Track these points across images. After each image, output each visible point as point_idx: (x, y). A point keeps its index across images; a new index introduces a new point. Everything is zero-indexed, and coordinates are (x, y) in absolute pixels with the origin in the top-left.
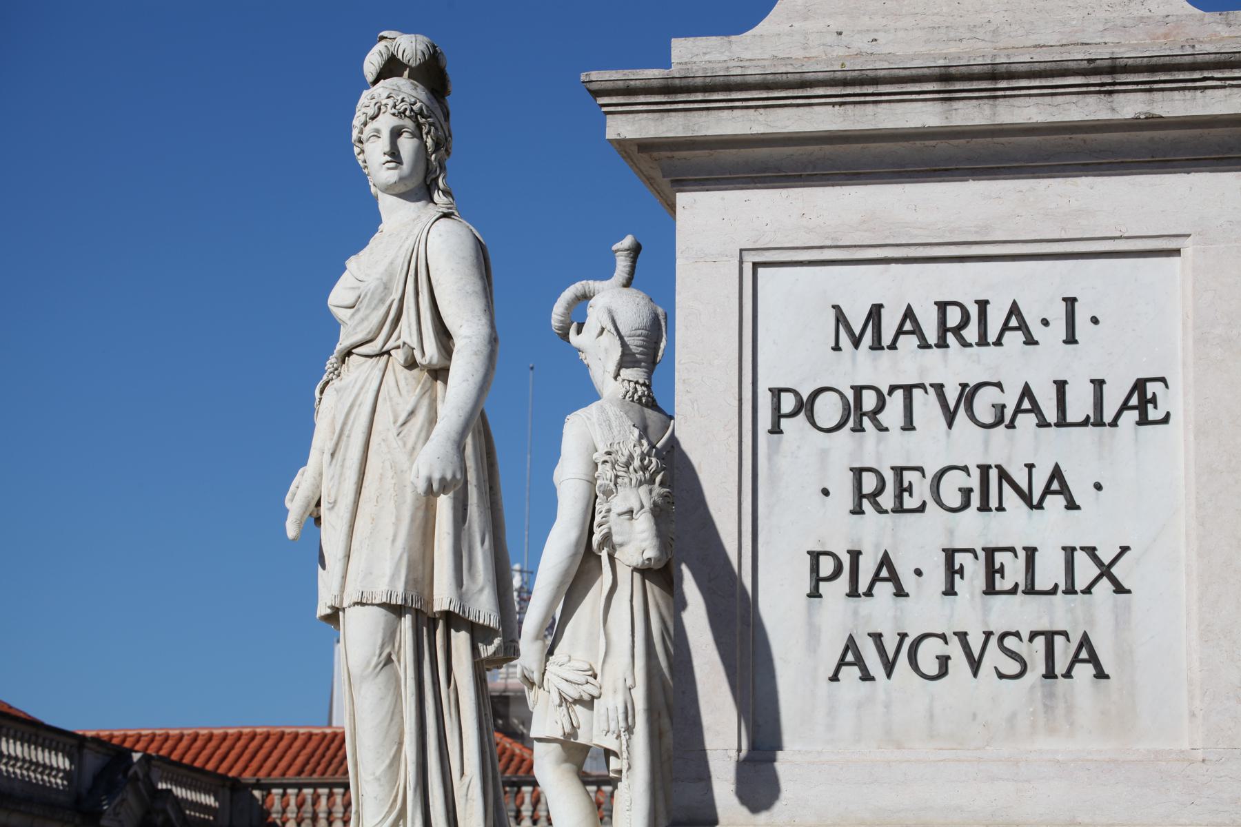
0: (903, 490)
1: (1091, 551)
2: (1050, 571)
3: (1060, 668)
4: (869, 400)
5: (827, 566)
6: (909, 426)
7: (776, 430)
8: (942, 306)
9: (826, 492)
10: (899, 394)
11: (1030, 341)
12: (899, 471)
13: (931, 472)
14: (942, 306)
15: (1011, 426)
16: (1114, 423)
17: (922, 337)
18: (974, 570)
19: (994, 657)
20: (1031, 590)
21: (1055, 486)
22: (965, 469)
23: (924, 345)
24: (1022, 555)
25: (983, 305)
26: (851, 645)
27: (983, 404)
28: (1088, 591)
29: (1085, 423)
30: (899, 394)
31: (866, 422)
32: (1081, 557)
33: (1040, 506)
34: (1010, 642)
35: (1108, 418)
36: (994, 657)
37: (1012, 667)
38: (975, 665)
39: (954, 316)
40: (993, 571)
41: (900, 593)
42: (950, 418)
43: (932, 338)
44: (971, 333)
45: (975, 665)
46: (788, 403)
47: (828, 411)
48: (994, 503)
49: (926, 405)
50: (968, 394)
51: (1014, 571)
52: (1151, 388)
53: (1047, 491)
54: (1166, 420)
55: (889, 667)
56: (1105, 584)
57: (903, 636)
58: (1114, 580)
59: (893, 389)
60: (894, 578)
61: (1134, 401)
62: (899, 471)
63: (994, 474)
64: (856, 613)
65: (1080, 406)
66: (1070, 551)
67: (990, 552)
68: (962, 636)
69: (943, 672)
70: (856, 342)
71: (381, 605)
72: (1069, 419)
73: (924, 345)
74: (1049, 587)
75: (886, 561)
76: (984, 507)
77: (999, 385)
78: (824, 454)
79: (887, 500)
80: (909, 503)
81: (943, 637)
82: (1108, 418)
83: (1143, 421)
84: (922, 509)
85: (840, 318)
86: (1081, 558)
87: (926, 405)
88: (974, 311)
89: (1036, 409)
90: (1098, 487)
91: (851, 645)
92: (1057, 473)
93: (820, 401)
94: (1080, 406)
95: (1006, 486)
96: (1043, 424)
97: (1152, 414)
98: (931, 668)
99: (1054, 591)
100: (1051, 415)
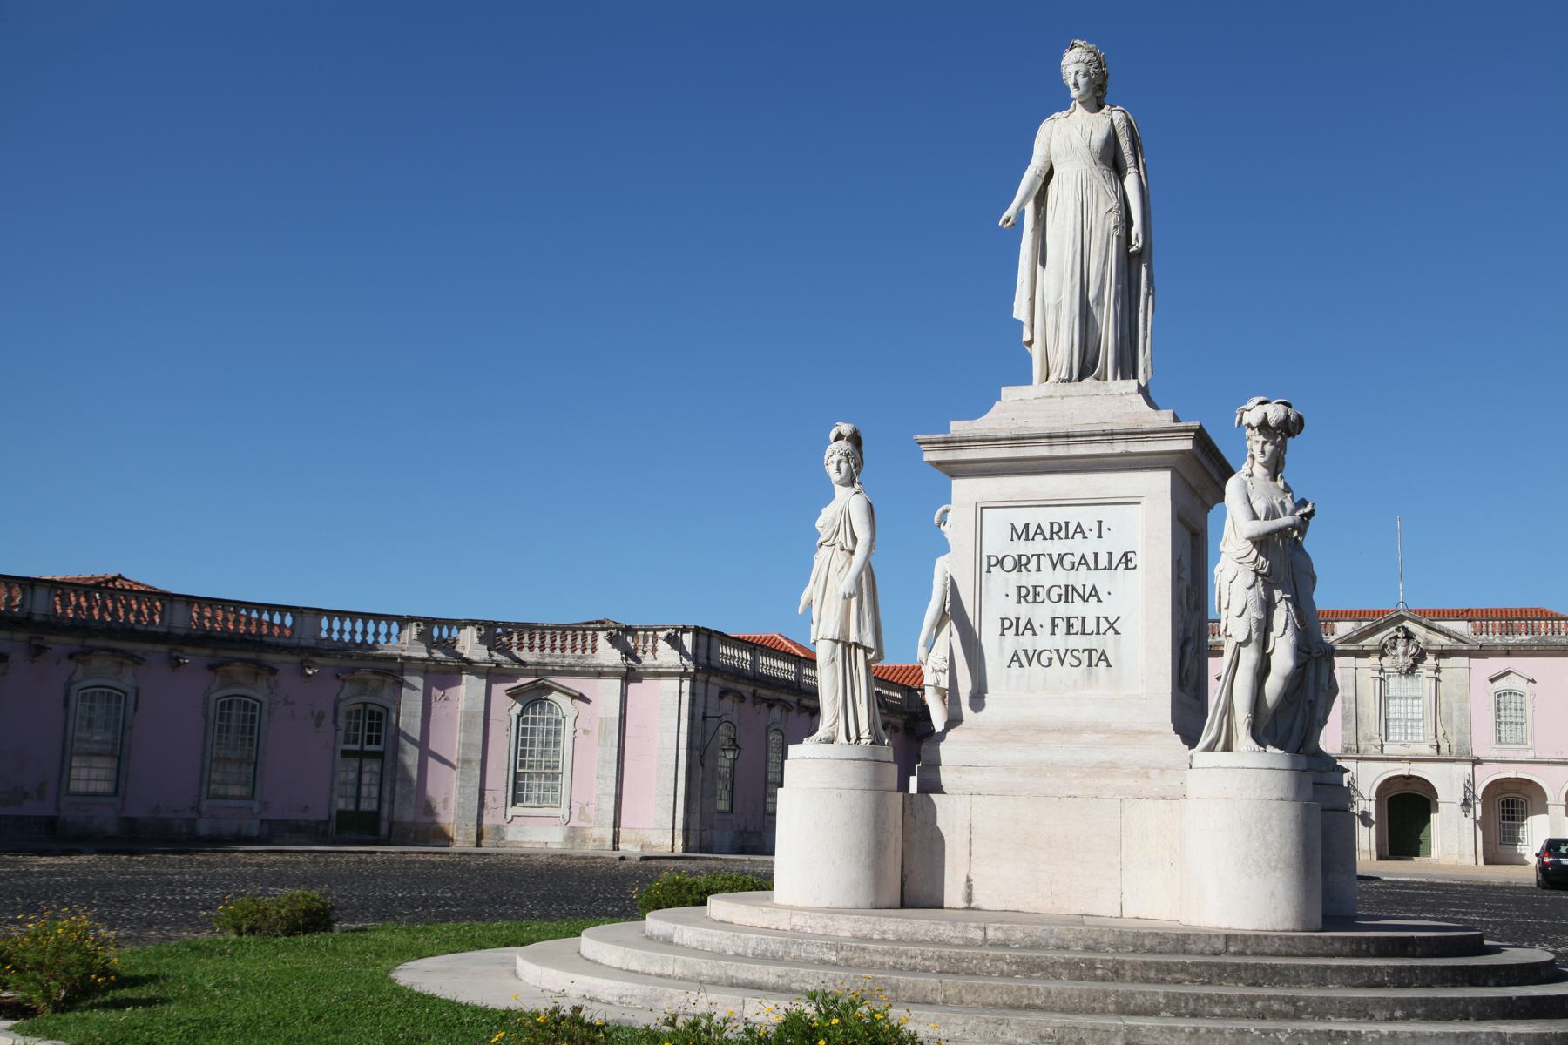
1: (1106, 618)
2: (1091, 626)
3: (1094, 663)
4: (1024, 560)
5: (1007, 624)
6: (1039, 570)
7: (989, 571)
8: (1052, 524)
9: (1007, 595)
10: (1035, 557)
11: (1085, 537)
12: (1035, 587)
13: (1047, 588)
14: (1052, 524)
15: (1077, 570)
16: (1116, 569)
17: (1044, 535)
18: (1062, 625)
19: (1069, 659)
20: (1083, 633)
21: (1093, 593)
22: (1060, 586)
23: (1045, 539)
24: (1080, 619)
25: (1067, 523)
26: (1016, 654)
27: (1067, 561)
28: (1105, 633)
29: (1105, 569)
30: (1035, 557)
31: (1023, 568)
33: (1087, 601)
34: (1075, 653)
35: (1113, 567)
36: (1069, 659)
37: (1076, 662)
38: (1062, 662)
39: (1056, 528)
41: (1034, 634)
42: (1054, 567)
43: (1048, 536)
44: (1062, 534)
45: (1062, 662)
46: (993, 561)
47: (1008, 564)
48: (1070, 600)
49: (1045, 562)
50: (1061, 558)
51: (1077, 625)
52: (1130, 555)
53: (1090, 595)
54: (1135, 568)
55: (1030, 662)
57: (1035, 650)
58: (1114, 629)
59: (1033, 556)
60: (1032, 628)
61: (1123, 560)
62: (1035, 587)
63: (1070, 588)
64: (1018, 641)
65: (1103, 562)
66: (1098, 618)
67: (1068, 619)
68: (1057, 651)
69: (1050, 664)
70: (1019, 538)
71: (831, 640)
73: (1045, 539)
75: (1029, 622)
77: (1073, 554)
78: (1007, 581)
79: (1030, 598)
80: (1038, 599)
82: (1113, 567)
83: (1127, 568)
84: (1043, 602)
85: (1013, 528)
86: (1103, 622)
87: (1045, 562)
88: (1064, 526)
89: (1086, 563)
90: (1109, 593)
91: (1016, 654)
92: (1094, 588)
93: (1005, 560)
94: (1103, 562)
95: (1075, 592)
96: (1089, 569)
97: (1130, 565)
99: (1092, 633)
100: (1092, 566)
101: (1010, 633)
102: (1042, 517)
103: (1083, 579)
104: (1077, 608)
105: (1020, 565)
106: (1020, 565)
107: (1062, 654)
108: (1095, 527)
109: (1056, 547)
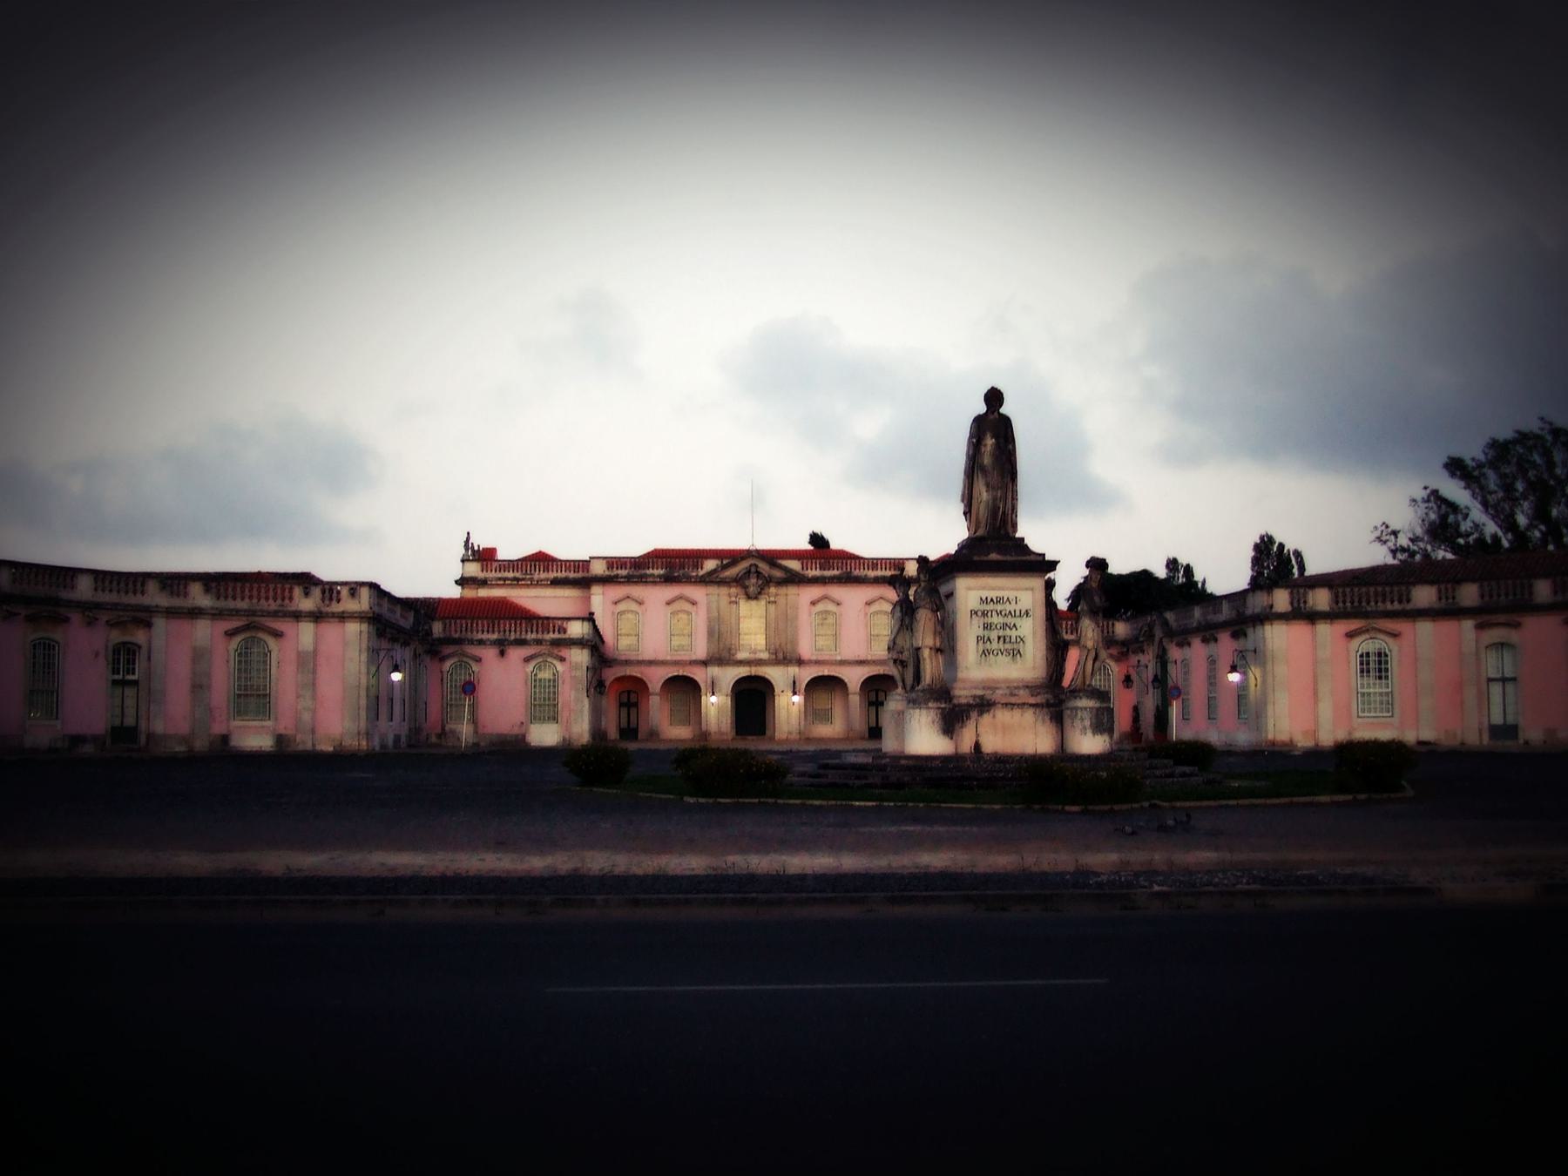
2: (1013, 640)
18: (1002, 639)
40: (1005, 640)
47: (979, 613)
49: (994, 613)
51: (1008, 640)
55: (989, 654)
65: (1018, 613)
85: (981, 599)
87: (994, 613)
94: (1018, 613)
102: (993, 594)
103: (1009, 620)
104: (1008, 632)
106: (984, 614)
109: (999, 607)
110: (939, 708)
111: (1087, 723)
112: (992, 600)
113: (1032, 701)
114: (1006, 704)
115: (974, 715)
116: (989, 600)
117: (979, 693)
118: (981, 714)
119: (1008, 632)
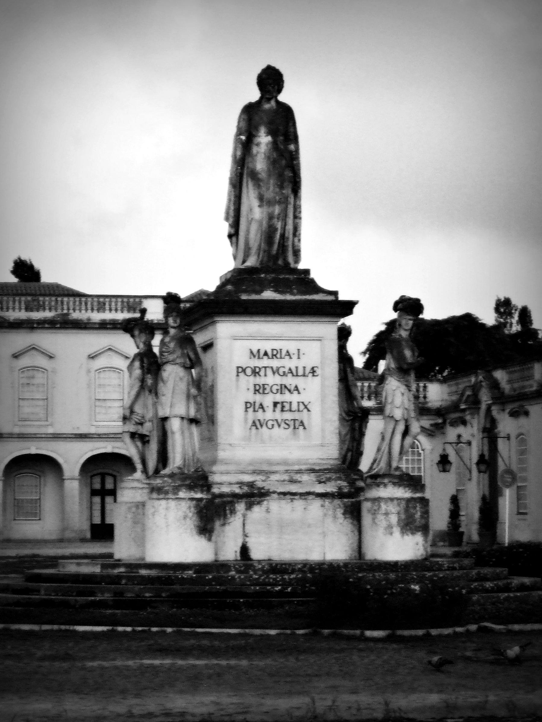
0: (264, 389)
2: (294, 407)
6: (265, 375)
8: (273, 350)
12: (263, 385)
13: (270, 385)
19: (283, 425)
20: (290, 410)
27: (281, 371)
32: (301, 404)
34: (287, 422)
37: (287, 427)
38: (279, 426)
40: (283, 407)
47: (249, 371)
50: (278, 369)
52: (315, 369)
55: (261, 426)
56: (305, 410)
63: (283, 386)
65: (301, 372)
67: (283, 402)
72: (299, 375)
73: (269, 358)
74: (295, 410)
76: (281, 393)
78: (248, 381)
79: (261, 391)
81: (272, 420)
83: (314, 376)
85: (252, 352)
87: (269, 372)
88: (279, 351)
89: (292, 373)
94: (301, 372)
97: (315, 374)
98: (270, 426)
100: (295, 373)
101: (251, 410)
102: (268, 346)
103: (290, 381)
104: (287, 397)
105: (255, 372)
106: (255, 372)
107: (279, 421)
108: (296, 352)
109: (275, 363)
110: (192, 499)
111: (394, 519)
112: (266, 354)
113: (320, 489)
114: (284, 494)
115: (241, 507)
116: (262, 353)
117: (247, 478)
118: (249, 507)
119: (287, 397)
